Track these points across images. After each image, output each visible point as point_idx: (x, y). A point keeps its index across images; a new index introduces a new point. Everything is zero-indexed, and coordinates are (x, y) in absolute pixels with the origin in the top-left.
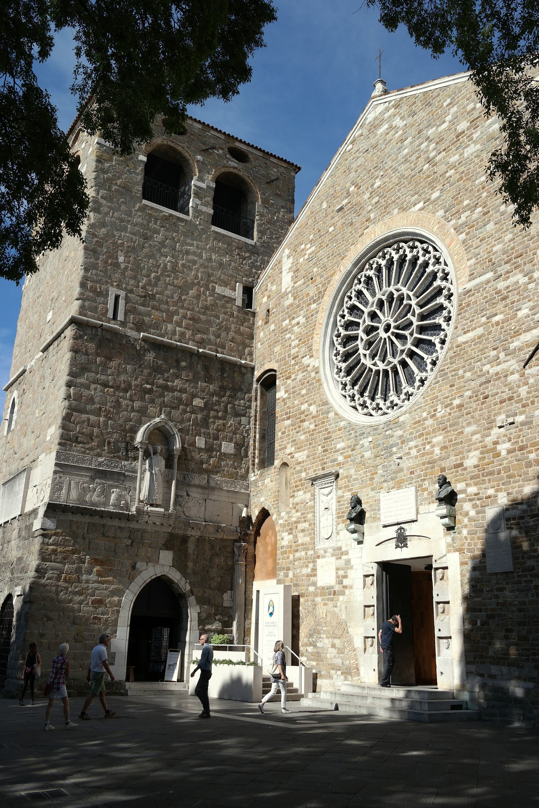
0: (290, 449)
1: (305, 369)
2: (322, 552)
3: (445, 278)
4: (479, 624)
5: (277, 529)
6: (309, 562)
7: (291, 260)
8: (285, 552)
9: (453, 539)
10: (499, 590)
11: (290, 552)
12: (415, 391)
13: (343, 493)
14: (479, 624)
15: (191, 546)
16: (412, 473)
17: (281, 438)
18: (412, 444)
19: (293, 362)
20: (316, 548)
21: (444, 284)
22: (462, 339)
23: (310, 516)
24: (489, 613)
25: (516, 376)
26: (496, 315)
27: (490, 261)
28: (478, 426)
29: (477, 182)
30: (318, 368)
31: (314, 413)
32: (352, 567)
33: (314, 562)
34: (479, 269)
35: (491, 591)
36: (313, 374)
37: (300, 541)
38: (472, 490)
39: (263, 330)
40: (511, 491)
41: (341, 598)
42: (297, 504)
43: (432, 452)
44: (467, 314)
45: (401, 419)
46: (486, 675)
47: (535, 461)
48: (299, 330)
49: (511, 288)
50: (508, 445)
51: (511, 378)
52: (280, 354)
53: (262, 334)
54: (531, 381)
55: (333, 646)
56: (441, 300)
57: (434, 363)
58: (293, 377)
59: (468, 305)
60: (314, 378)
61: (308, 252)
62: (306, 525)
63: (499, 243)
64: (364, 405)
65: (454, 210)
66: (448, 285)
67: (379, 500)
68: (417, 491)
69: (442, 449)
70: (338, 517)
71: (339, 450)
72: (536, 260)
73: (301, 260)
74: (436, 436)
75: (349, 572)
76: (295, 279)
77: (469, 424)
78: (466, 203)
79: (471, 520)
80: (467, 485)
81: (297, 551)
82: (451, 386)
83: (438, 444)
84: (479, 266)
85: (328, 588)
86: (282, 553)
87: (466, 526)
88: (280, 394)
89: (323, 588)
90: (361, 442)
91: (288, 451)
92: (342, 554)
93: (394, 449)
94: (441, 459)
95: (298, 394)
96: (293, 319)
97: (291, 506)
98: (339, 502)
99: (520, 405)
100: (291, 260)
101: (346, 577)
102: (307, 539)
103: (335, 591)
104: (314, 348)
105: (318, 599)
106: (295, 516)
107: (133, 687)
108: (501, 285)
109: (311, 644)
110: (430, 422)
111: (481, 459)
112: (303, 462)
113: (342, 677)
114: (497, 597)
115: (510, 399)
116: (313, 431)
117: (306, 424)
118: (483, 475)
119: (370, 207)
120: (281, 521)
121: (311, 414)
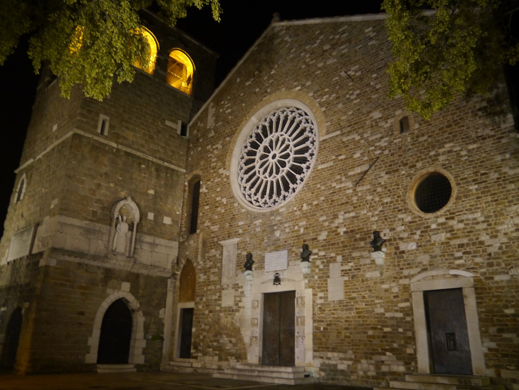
0: (207, 224)
1: (220, 176)
2: (226, 286)
3: (311, 131)
4: (322, 329)
5: (197, 271)
6: (217, 292)
7: (214, 109)
8: (201, 286)
9: (309, 281)
10: (334, 310)
11: (204, 286)
12: (289, 195)
13: (242, 251)
14: (322, 329)
15: (142, 281)
16: (286, 242)
17: (202, 216)
18: (286, 225)
19: (212, 171)
20: (222, 284)
21: (310, 135)
22: (320, 167)
23: (219, 265)
24: (328, 323)
25: (351, 191)
26: (341, 155)
27: (339, 124)
28: (327, 217)
29: (334, 80)
30: (228, 176)
31: (225, 203)
32: (245, 296)
33: (220, 292)
34: (332, 128)
35: (330, 310)
36: (225, 180)
37: (211, 279)
38: (322, 253)
39: (193, 149)
40: (344, 255)
41: (237, 314)
42: (211, 257)
43: (299, 231)
44: (324, 153)
45: (281, 210)
46: (325, 358)
47: (359, 238)
48: (218, 152)
49: (350, 141)
50: (345, 229)
51: (348, 192)
52: (204, 166)
53: (192, 153)
54: (360, 194)
55: (230, 342)
56: (308, 144)
57: (302, 180)
58: (212, 180)
59: (325, 148)
60: (226, 182)
61: (226, 106)
62: (216, 270)
63: (344, 115)
64: (257, 201)
65: (319, 93)
66: (313, 136)
67: (264, 257)
68: (289, 252)
69: (305, 229)
70: (238, 266)
71: (240, 226)
72: (365, 127)
73: (221, 110)
74: (301, 221)
75: (243, 299)
76: (216, 121)
77: (322, 216)
78: (326, 90)
79: (320, 270)
80: (319, 250)
81: (208, 285)
82: (313, 193)
83: (303, 226)
84: (332, 126)
85: (228, 307)
86: (199, 286)
87: (317, 274)
88: (203, 190)
89: (225, 308)
90: (255, 223)
91: (206, 225)
92: (239, 287)
93: (275, 228)
94: (303, 234)
95: (215, 191)
96: (214, 145)
97: (206, 258)
98: (238, 257)
99: (352, 207)
100: (214, 109)
101: (240, 301)
102: (216, 278)
103: (233, 311)
104: (226, 164)
105: (222, 314)
106: (209, 264)
107: (103, 369)
108: (345, 139)
109: (216, 341)
110: (298, 213)
111: (328, 236)
112: (216, 232)
113: (235, 361)
114: (333, 314)
115: (347, 203)
116: (223, 213)
117: (219, 209)
118: (329, 245)
119: (267, 85)
120: (199, 267)
121: (223, 203)
